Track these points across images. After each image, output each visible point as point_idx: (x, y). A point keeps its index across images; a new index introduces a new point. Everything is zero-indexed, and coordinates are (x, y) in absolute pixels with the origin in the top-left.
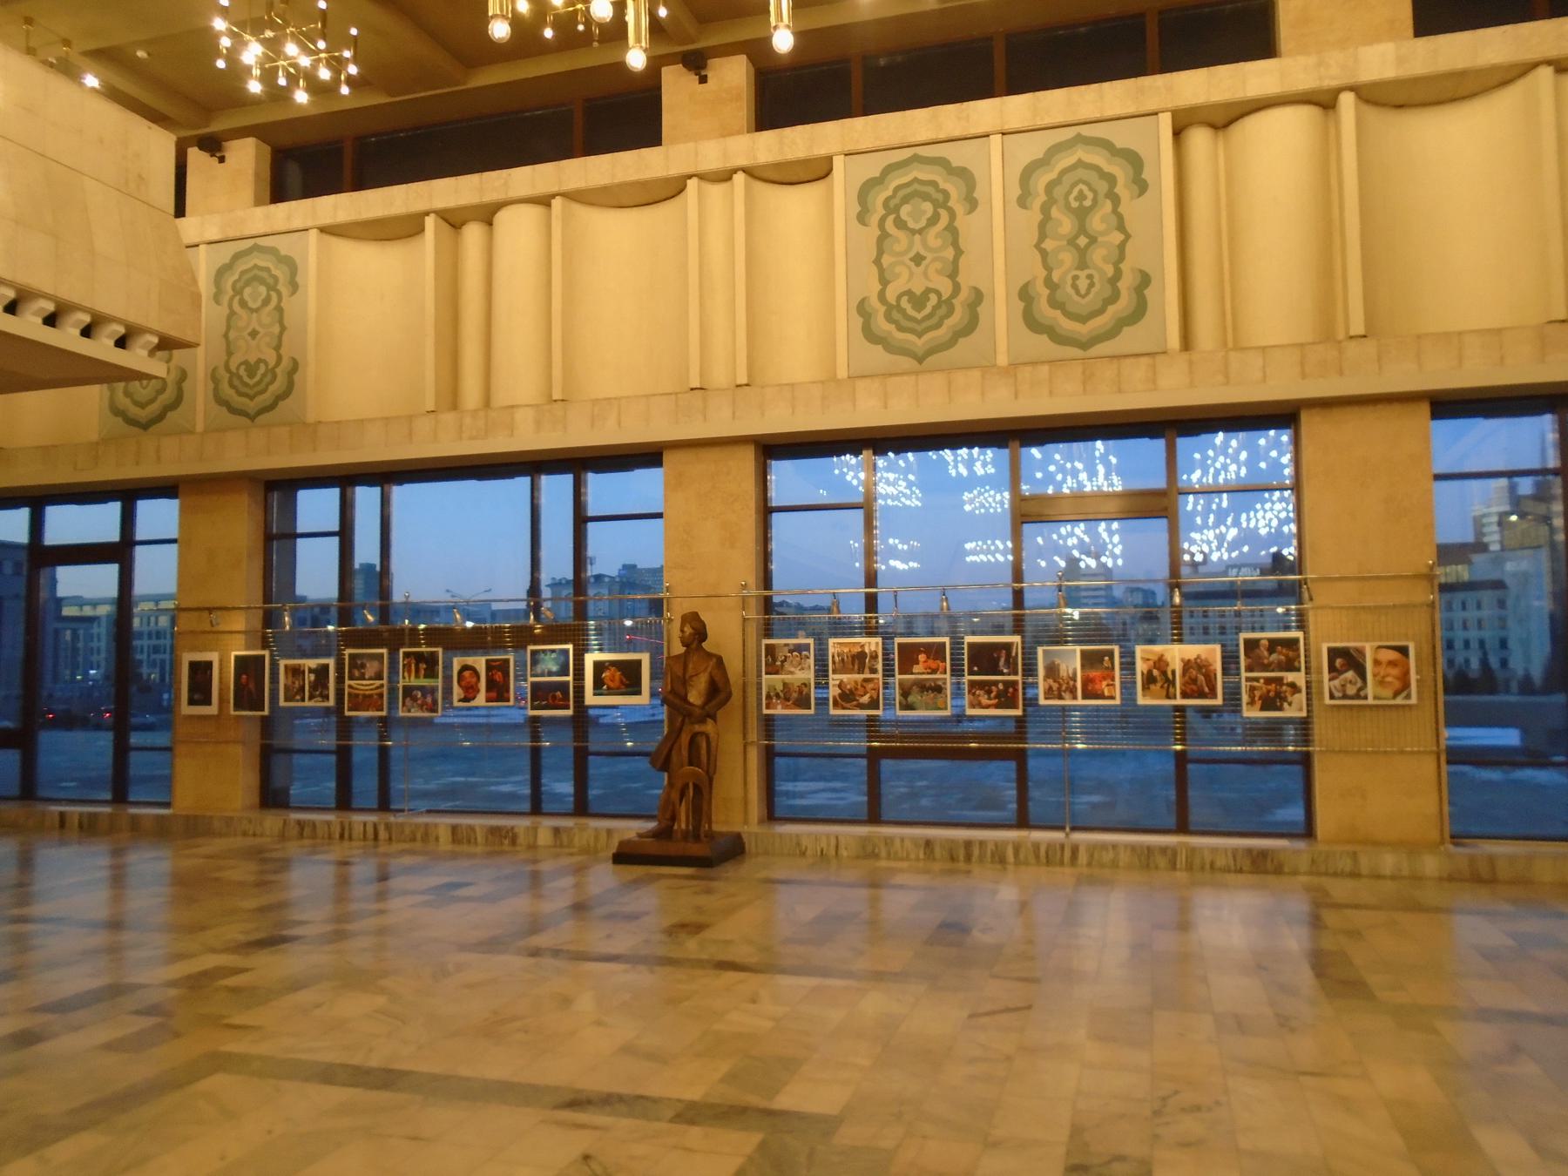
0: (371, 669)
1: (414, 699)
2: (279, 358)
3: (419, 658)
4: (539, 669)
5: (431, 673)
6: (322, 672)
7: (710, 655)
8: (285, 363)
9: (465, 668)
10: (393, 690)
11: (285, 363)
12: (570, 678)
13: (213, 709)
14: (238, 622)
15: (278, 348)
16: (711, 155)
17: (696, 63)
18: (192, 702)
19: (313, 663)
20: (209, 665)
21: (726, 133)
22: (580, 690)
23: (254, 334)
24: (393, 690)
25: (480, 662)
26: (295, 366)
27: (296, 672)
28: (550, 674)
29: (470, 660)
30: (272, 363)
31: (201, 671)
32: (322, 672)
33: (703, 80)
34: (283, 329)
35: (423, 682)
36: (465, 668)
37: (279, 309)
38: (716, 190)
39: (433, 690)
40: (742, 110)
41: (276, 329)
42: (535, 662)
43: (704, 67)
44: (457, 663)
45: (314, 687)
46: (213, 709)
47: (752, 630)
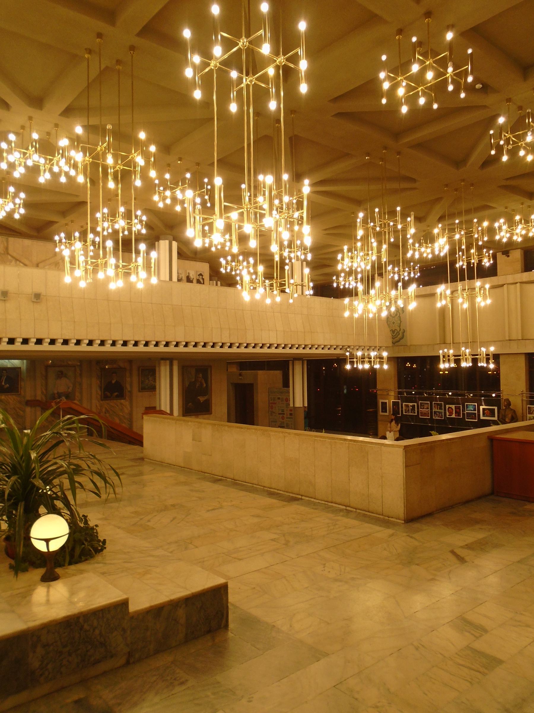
0: (426, 406)
1: (437, 414)
2: (400, 330)
3: (438, 404)
4: (468, 409)
5: (441, 409)
6: (414, 406)
7: (512, 409)
8: (402, 330)
9: (449, 408)
10: (431, 412)
11: (402, 330)
12: (476, 412)
13: (387, 414)
14: (392, 393)
15: (400, 326)
16: (510, 279)
17: (506, 253)
18: (382, 412)
19: (411, 404)
20: (386, 403)
21: (516, 272)
22: (479, 415)
23: (394, 323)
24: (431, 412)
25: (453, 407)
26: (404, 331)
27: (407, 406)
28: (471, 410)
29: (451, 406)
30: (398, 330)
31: (384, 405)
32: (414, 406)
33: (508, 256)
34: (401, 322)
35: (439, 410)
36: (449, 408)
37: (399, 317)
38: (512, 287)
39: (441, 413)
40: (519, 265)
41: (399, 322)
42: (467, 407)
43: (508, 253)
44: (447, 406)
45: (412, 410)
46: (387, 414)
47: (525, 403)
